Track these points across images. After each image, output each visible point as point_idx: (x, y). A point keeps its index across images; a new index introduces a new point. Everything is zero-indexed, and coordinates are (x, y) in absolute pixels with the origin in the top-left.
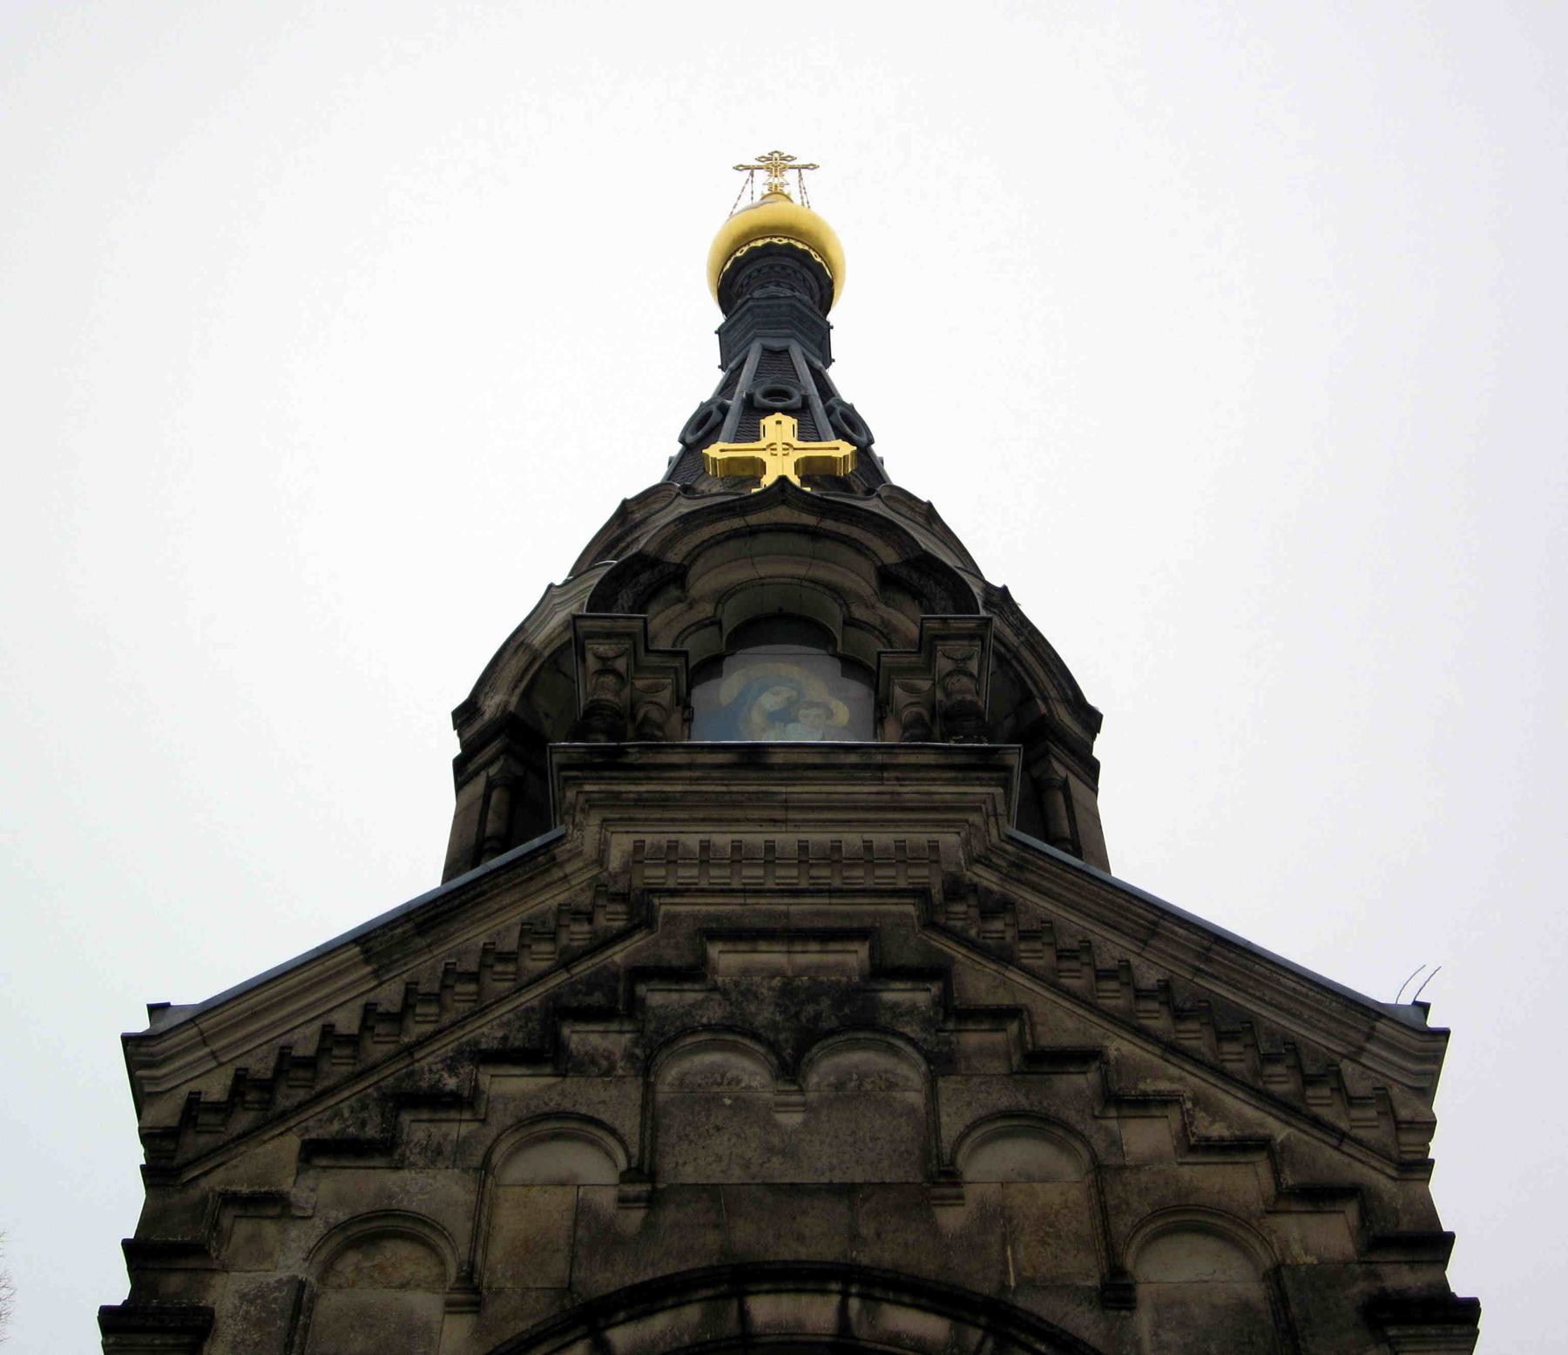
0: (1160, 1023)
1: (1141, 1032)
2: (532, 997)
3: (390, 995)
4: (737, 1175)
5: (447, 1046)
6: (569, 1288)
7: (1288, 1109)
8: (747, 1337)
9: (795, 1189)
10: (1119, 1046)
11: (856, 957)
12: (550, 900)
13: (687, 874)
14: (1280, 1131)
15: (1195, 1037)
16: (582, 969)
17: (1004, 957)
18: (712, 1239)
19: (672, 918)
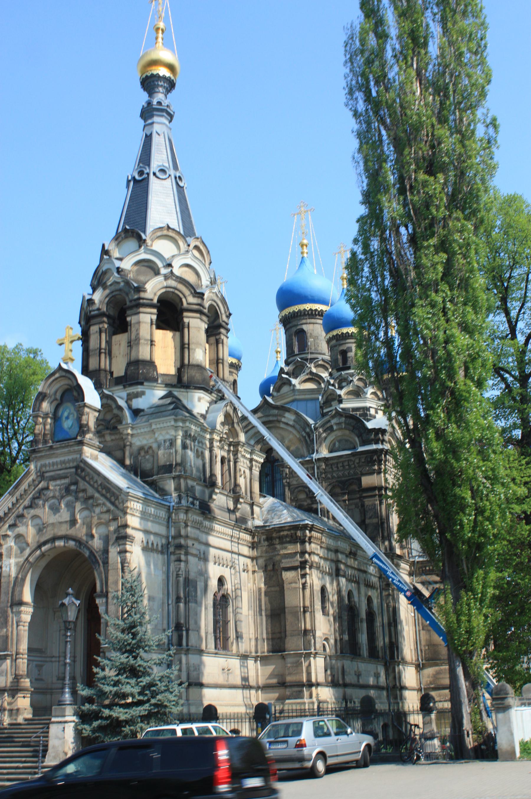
0: (100, 489)
1: (98, 492)
2: (31, 496)
3: (14, 500)
4: (55, 521)
5: (22, 506)
6: (38, 542)
7: (113, 504)
8: (55, 547)
9: (61, 523)
10: (97, 495)
11: (67, 481)
12: (31, 479)
13: (48, 469)
14: (112, 508)
15: (104, 492)
16: (36, 489)
17: (84, 479)
18: (52, 532)
19: (47, 477)
